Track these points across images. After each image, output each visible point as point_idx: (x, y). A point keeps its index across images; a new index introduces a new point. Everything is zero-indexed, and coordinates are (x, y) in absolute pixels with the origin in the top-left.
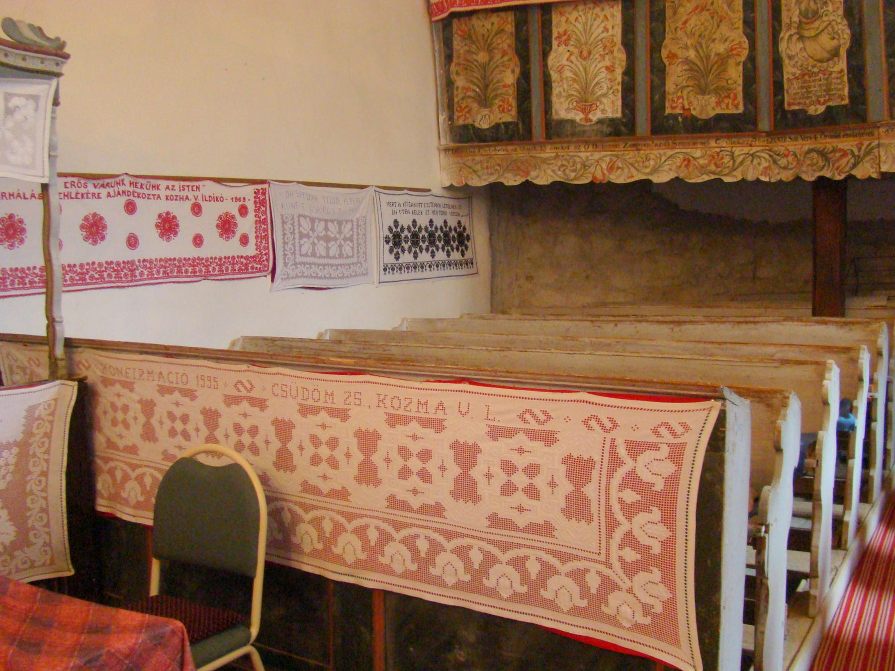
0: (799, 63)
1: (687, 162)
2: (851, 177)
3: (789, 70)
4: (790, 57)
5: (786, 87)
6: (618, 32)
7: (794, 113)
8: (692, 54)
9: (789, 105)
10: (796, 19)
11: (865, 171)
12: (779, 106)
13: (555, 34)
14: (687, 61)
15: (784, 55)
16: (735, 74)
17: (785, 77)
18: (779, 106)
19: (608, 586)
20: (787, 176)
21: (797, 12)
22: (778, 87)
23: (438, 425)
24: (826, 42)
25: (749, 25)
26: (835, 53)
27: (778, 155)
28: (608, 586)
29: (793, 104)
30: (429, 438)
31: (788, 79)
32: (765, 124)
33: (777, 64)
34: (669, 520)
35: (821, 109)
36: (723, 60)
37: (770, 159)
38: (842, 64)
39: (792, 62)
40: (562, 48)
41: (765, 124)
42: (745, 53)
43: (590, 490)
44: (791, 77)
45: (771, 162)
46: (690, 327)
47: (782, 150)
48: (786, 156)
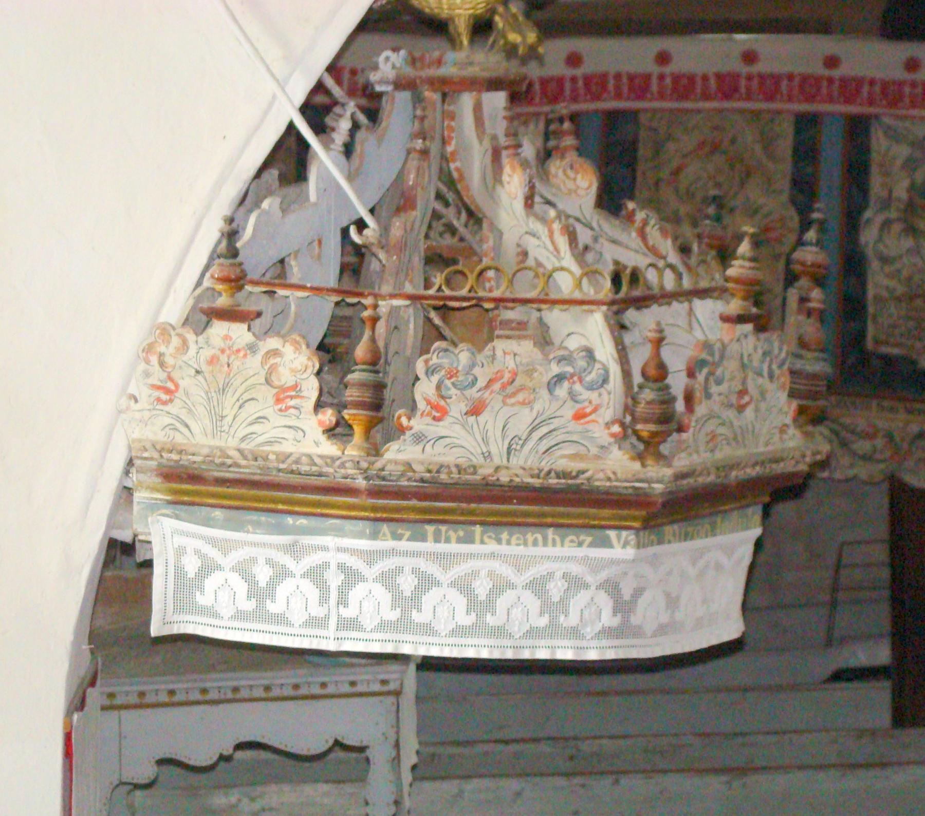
0: (905, 273)
4: (885, 260)
5: (871, 310)
7: (887, 360)
9: (877, 342)
10: (901, 191)
15: (870, 252)
17: (871, 292)
21: (906, 183)
27: (853, 432)
29: (887, 343)
31: (878, 299)
37: (833, 437)
39: (887, 269)
44: (884, 293)
45: (836, 442)
46: (762, 778)
47: (862, 424)
48: (871, 436)
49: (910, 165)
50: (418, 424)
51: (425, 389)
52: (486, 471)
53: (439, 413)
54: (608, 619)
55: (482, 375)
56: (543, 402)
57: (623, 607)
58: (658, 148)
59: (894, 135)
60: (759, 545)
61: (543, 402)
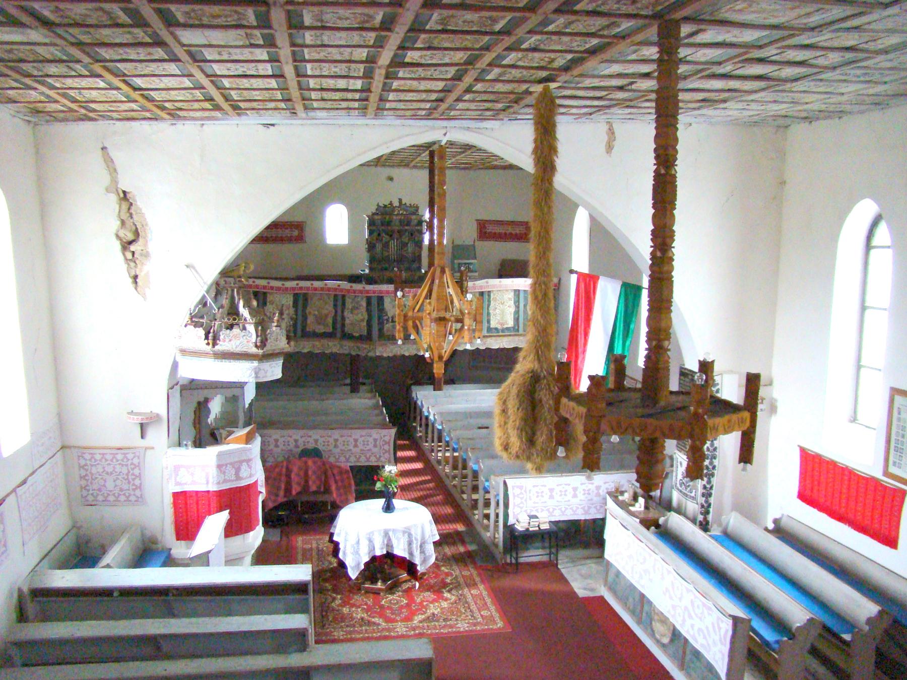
1: (314, 346)
2: (367, 356)
3: (347, 322)
6: (291, 303)
8: (316, 313)
10: (350, 307)
11: (371, 354)
12: (343, 331)
13: (268, 300)
14: (314, 315)
16: (330, 320)
18: (343, 331)
19: (380, 457)
20: (346, 352)
22: (343, 325)
23: (351, 436)
24: (360, 317)
25: (335, 306)
26: (362, 320)
28: (380, 457)
30: (349, 438)
32: (338, 335)
33: (343, 318)
34: (389, 446)
35: (357, 335)
36: (326, 316)
38: (365, 324)
40: (271, 306)
41: (338, 335)
42: (333, 314)
43: (378, 443)
49: (352, 303)
50: (221, 343)
51: (222, 337)
52: (232, 350)
53: (224, 341)
54: (253, 375)
55: (231, 335)
56: (241, 339)
57: (256, 373)
58: (311, 299)
59: (349, 298)
60: (283, 364)
61: (241, 339)
